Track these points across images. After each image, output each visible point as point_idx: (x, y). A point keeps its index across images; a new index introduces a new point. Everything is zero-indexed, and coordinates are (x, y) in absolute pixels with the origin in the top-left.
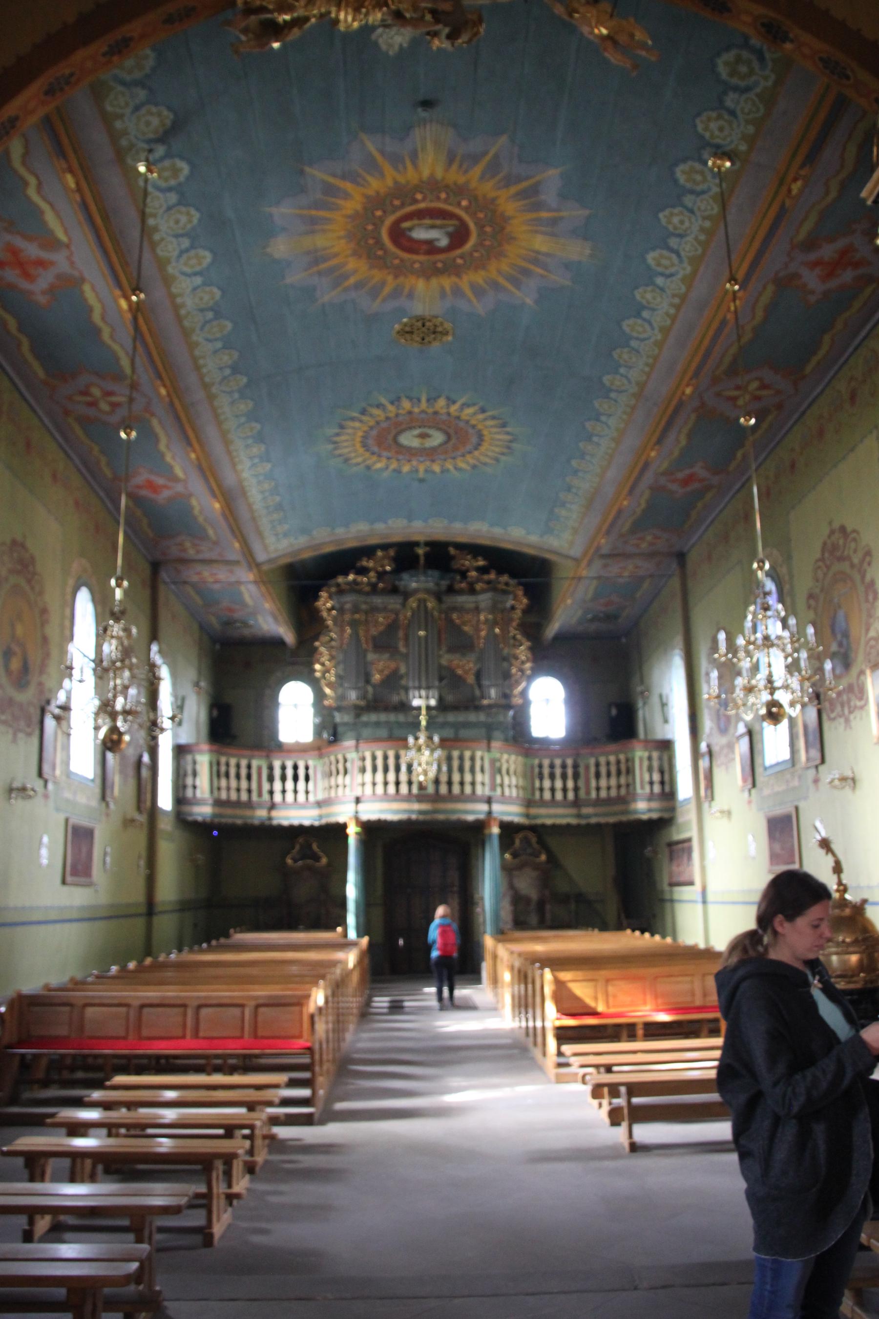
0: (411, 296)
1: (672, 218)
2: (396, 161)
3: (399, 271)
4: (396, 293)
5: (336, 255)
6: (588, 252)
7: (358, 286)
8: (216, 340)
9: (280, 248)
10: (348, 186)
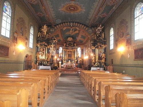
4: (75, 4)
7: (79, 5)
9: (84, 10)
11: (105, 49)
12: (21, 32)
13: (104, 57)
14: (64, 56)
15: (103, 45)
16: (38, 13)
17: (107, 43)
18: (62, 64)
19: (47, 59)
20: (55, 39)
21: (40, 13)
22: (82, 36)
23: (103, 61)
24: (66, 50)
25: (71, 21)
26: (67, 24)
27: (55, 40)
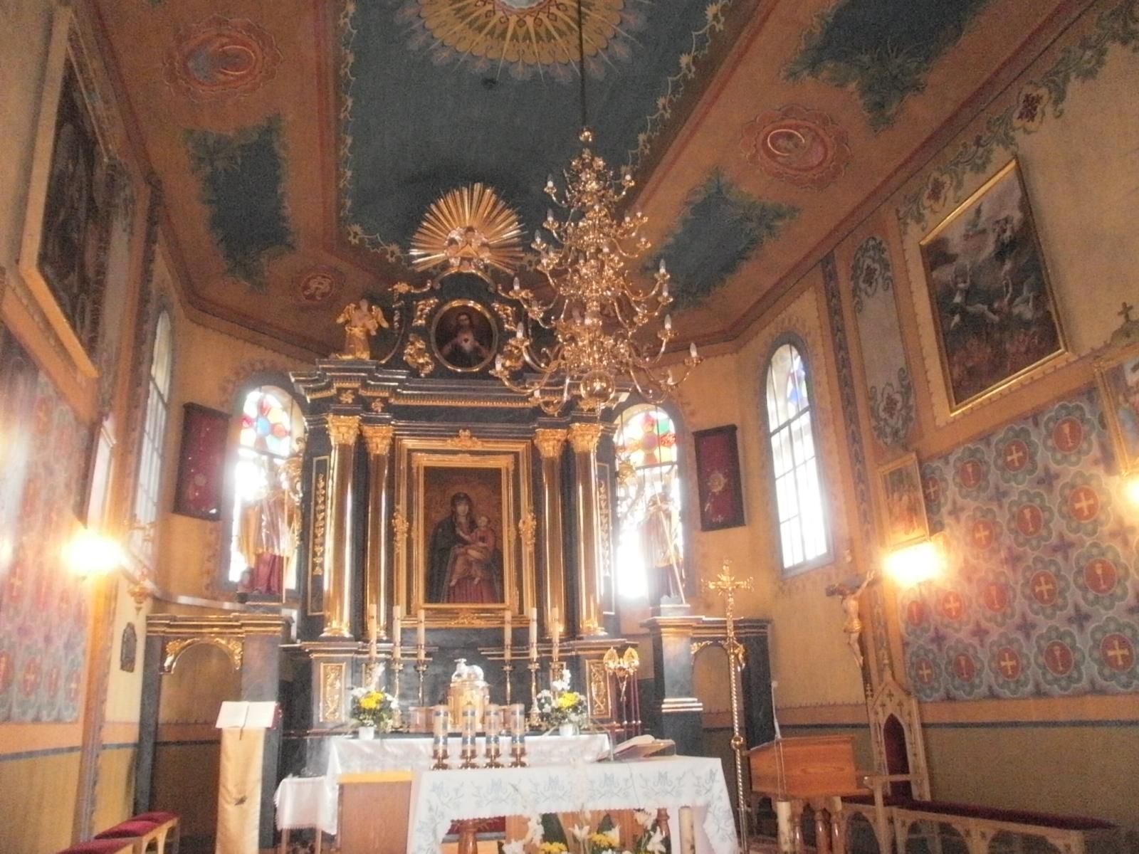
18: (291, 750)
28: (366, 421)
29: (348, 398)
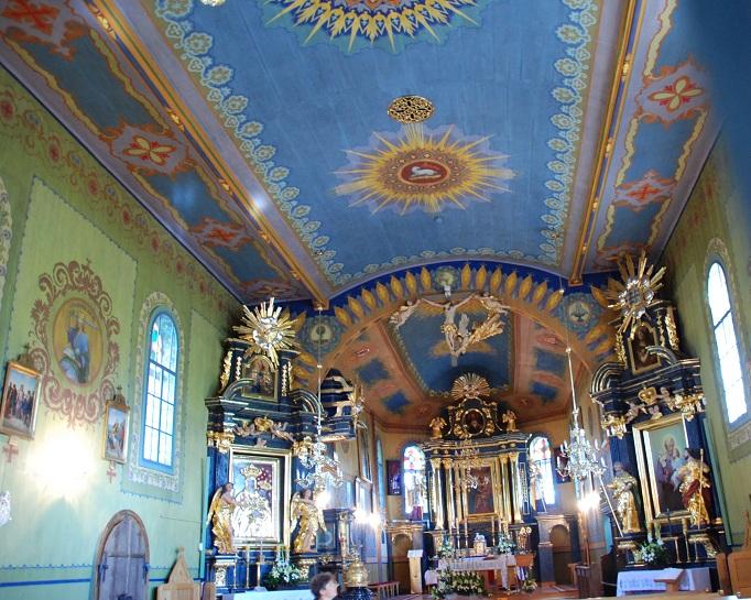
0: (427, 138)
1: (314, 226)
2: (448, 200)
3: (438, 154)
4: (437, 139)
5: (477, 163)
6: (337, 192)
7: (462, 145)
8: (562, 139)
9: (508, 174)
10: (469, 191)
11: (697, 426)
12: (66, 357)
13: (696, 484)
14: (439, 510)
15: (679, 399)
16: (208, 230)
17: (705, 375)
18: (427, 564)
19: (294, 536)
20: (347, 388)
21: (220, 227)
22: (540, 353)
23: (695, 512)
24: (448, 467)
25: (444, 257)
26: (419, 284)
27: (344, 397)
28: (442, 458)
29: (436, 452)
